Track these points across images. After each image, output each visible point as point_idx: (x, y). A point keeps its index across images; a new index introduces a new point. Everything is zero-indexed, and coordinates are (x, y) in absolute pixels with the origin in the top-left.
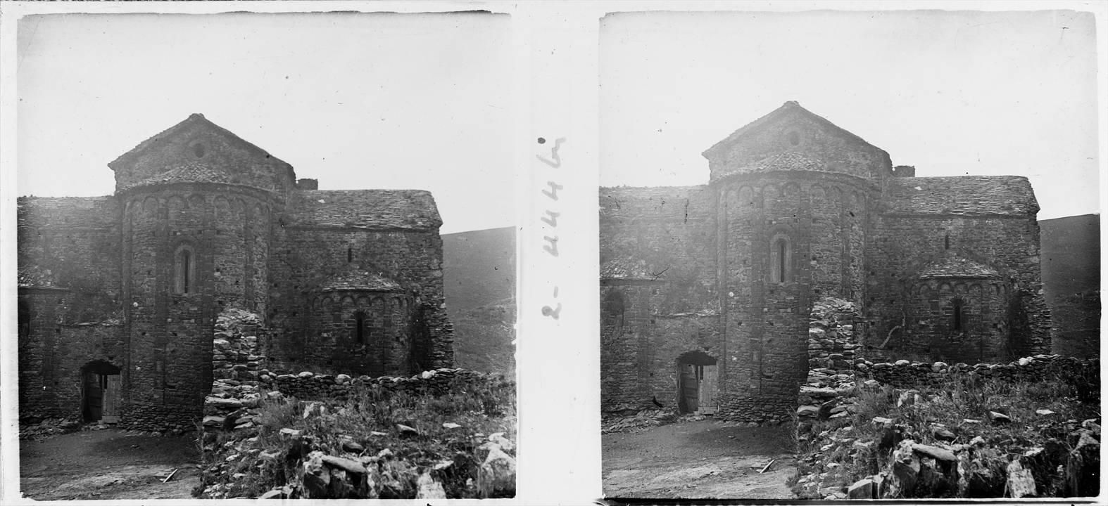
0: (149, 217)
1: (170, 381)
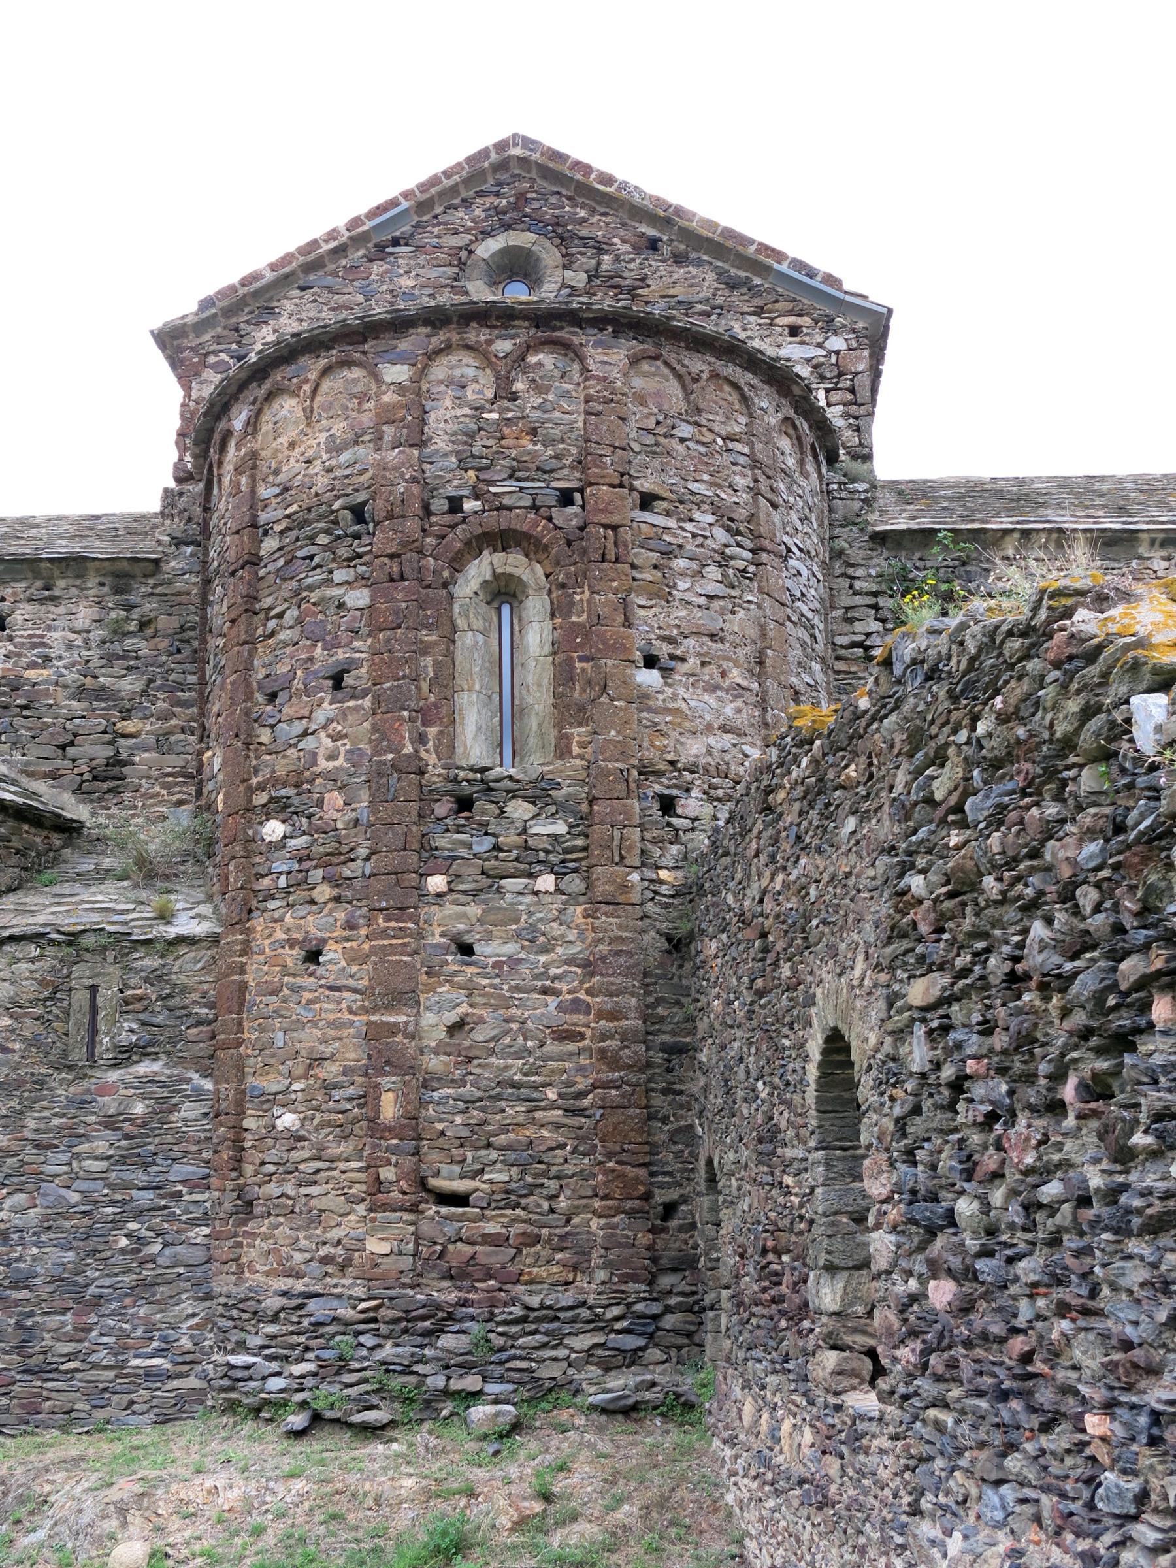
0: (335, 448)
1: (445, 1169)
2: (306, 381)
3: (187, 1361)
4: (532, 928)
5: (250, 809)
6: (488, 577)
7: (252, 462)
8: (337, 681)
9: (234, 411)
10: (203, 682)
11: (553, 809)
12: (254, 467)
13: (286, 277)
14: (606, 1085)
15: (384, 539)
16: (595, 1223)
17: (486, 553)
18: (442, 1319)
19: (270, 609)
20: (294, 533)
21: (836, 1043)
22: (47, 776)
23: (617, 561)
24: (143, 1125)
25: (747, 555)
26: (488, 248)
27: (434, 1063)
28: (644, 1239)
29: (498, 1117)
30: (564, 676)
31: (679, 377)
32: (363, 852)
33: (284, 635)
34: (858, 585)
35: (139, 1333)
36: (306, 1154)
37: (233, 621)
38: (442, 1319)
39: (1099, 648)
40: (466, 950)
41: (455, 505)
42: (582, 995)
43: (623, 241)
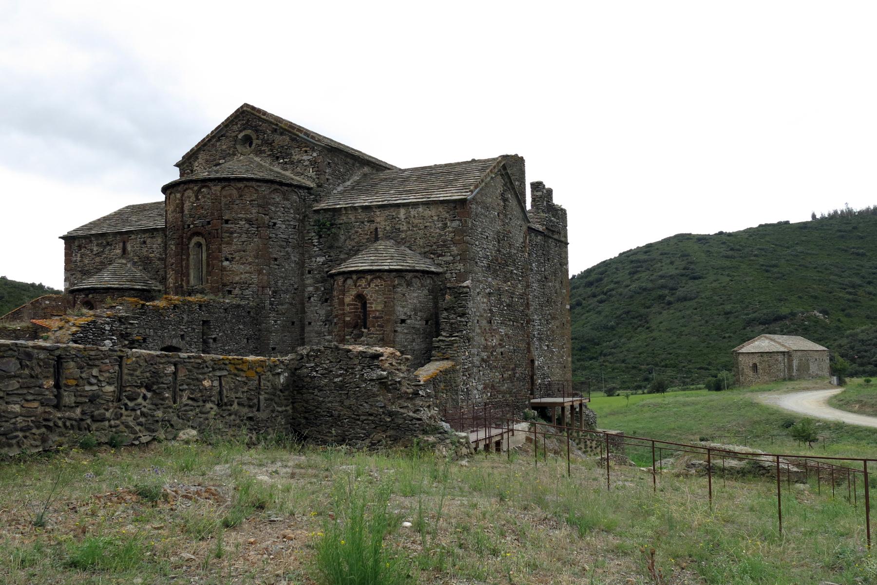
26: (240, 137)
30: (208, 265)
41: (189, 226)
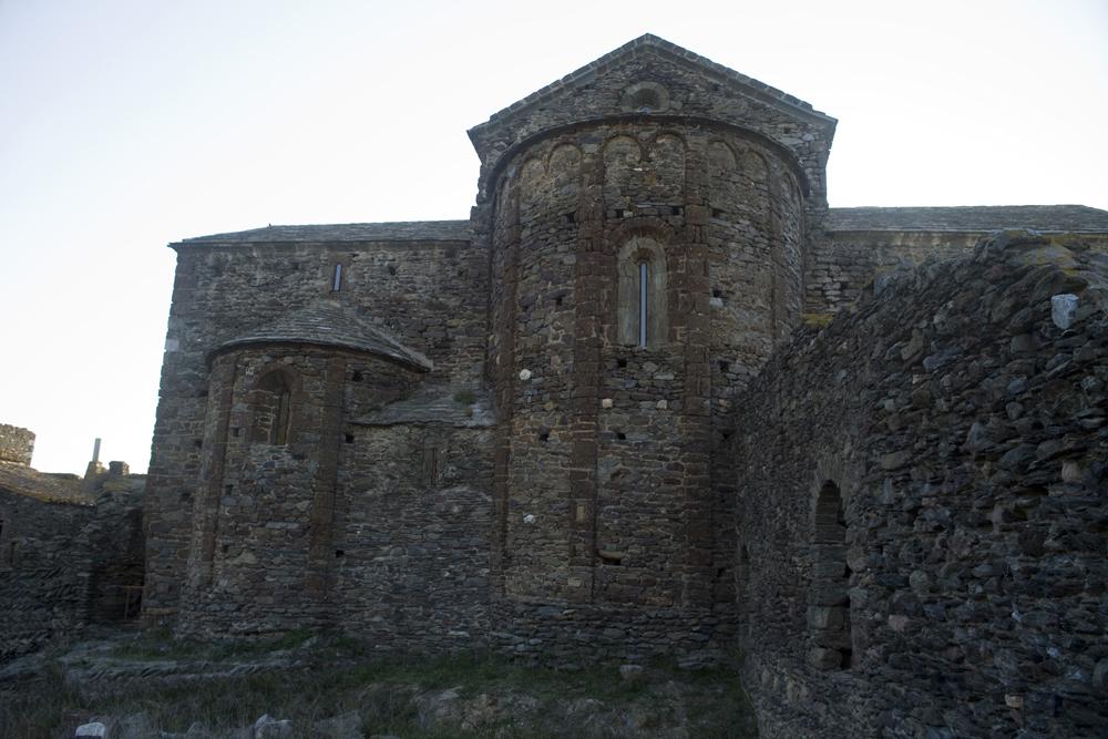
0: (559, 185)
2: (546, 152)
3: (476, 633)
4: (655, 427)
5: (513, 363)
6: (635, 249)
7: (516, 194)
8: (559, 301)
9: (509, 166)
10: (489, 301)
11: (666, 367)
12: (519, 195)
13: (533, 104)
14: (691, 507)
15: (584, 230)
16: (684, 577)
17: (634, 238)
18: (607, 620)
19: (526, 264)
20: (538, 228)
21: (830, 489)
22: (413, 345)
23: (701, 242)
24: (458, 518)
25: (766, 242)
26: (636, 88)
27: (604, 493)
28: (708, 586)
29: (636, 521)
31: (733, 151)
32: (570, 386)
33: (533, 278)
34: (819, 259)
35: (454, 618)
36: (538, 536)
37: (506, 271)
38: (607, 620)
39: (1026, 271)
40: (622, 437)
41: (619, 213)
42: (679, 461)
43: (701, 86)
